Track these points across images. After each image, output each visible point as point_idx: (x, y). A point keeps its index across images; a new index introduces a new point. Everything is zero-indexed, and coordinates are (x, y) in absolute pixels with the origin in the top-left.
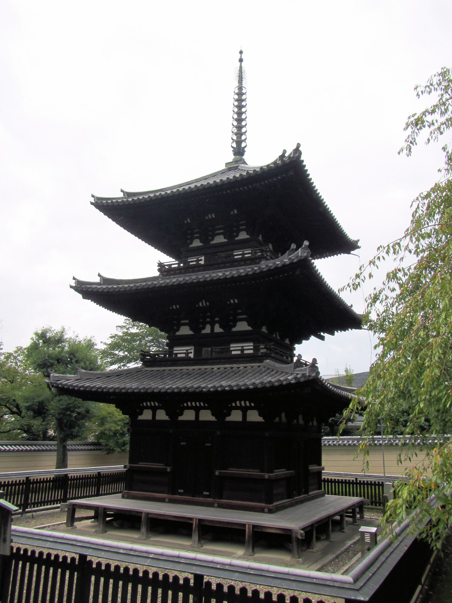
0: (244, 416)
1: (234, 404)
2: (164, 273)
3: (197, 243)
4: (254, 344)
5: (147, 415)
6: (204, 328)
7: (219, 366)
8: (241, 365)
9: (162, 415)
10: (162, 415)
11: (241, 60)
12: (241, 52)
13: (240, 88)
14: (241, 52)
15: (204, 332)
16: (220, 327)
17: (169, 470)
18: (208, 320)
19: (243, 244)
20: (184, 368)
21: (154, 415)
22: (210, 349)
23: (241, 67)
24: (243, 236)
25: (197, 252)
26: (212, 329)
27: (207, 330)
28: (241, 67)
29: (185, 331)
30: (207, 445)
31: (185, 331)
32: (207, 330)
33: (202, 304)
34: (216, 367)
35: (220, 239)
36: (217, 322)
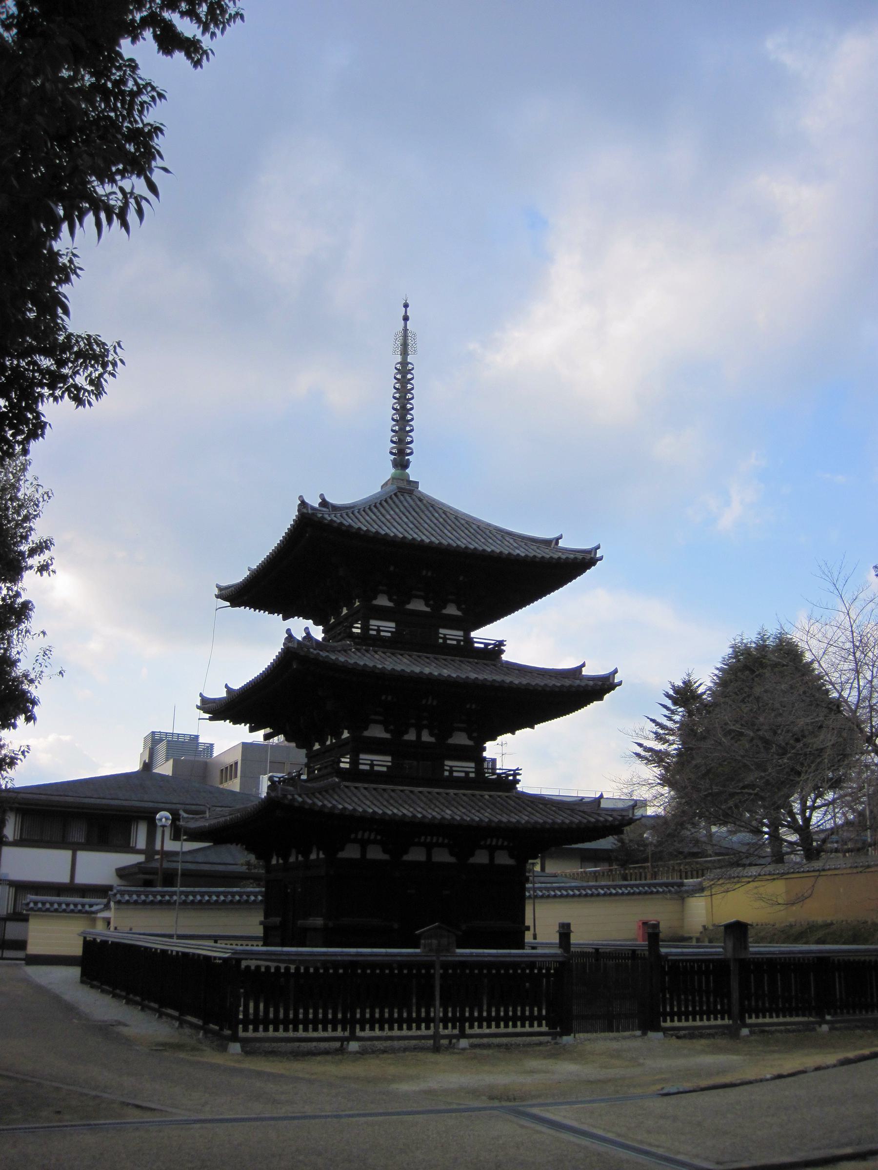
0: (492, 858)
1: (482, 843)
2: (357, 640)
3: (383, 601)
4: (475, 765)
5: (351, 852)
6: (407, 732)
7: (456, 791)
8: (485, 793)
9: (375, 853)
10: (375, 853)
11: (406, 318)
12: (406, 306)
13: (404, 363)
14: (406, 306)
15: (406, 737)
16: (431, 735)
17: (396, 926)
18: (413, 721)
20: (405, 788)
22: (415, 763)
23: (405, 330)
24: (452, 610)
25: (383, 614)
26: (419, 736)
27: (411, 736)
28: (405, 330)
32: (411, 736)
34: (452, 792)
35: (418, 605)
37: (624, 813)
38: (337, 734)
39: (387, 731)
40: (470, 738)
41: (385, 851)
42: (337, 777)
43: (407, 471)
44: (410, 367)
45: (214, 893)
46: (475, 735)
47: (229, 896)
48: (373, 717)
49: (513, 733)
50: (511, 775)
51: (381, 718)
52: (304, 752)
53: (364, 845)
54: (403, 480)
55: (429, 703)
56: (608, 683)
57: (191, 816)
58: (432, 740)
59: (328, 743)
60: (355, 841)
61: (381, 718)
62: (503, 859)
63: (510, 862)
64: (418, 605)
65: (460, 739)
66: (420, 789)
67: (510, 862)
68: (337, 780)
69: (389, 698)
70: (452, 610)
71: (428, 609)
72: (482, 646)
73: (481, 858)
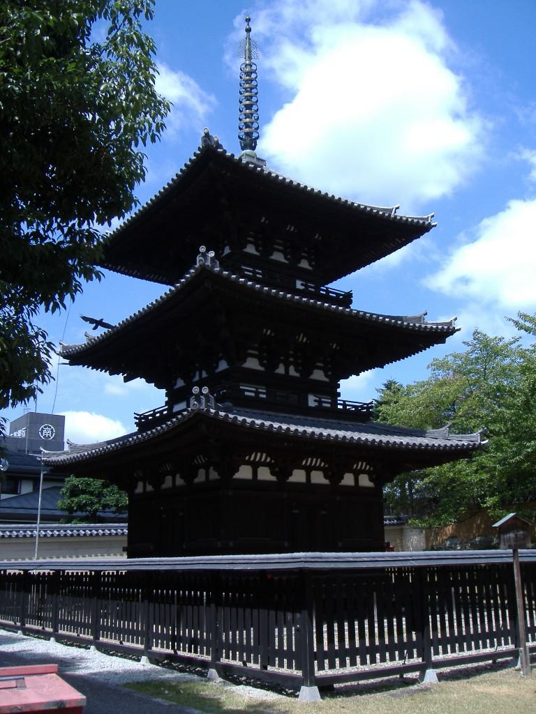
3: (250, 249)
6: (277, 367)
10: (265, 474)
16: (296, 370)
18: (282, 358)
19: (303, 275)
21: (255, 473)
24: (304, 264)
26: (287, 370)
27: (281, 370)
29: (252, 364)
30: (323, 512)
31: (252, 364)
32: (281, 370)
33: (302, 339)
35: (278, 257)
36: (291, 363)
37: (473, 439)
38: (211, 367)
39: (261, 364)
40: (326, 376)
41: (272, 473)
42: (231, 402)
43: (255, 151)
44: (254, 67)
45: (49, 528)
46: (330, 373)
47: (62, 531)
48: (250, 351)
49: (358, 375)
50: (364, 408)
51: (256, 352)
52: (164, 391)
53: (255, 466)
54: (254, 157)
55: (300, 340)
56: (451, 328)
57: (51, 452)
58: (297, 375)
59: (197, 378)
60: (248, 463)
61: (256, 352)
62: (365, 481)
63: (371, 484)
64: (278, 257)
65: (318, 375)
66: (298, 417)
67: (371, 484)
68: (230, 404)
69: (269, 332)
70: (304, 264)
71: (287, 262)
72: (335, 295)
73: (348, 480)
